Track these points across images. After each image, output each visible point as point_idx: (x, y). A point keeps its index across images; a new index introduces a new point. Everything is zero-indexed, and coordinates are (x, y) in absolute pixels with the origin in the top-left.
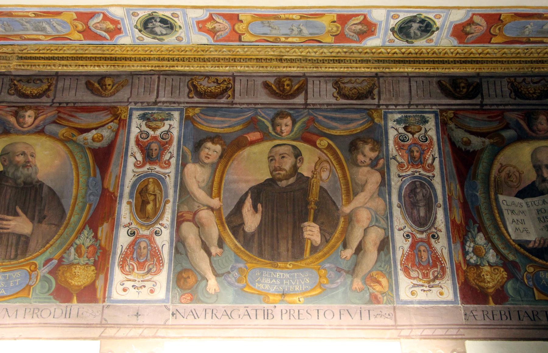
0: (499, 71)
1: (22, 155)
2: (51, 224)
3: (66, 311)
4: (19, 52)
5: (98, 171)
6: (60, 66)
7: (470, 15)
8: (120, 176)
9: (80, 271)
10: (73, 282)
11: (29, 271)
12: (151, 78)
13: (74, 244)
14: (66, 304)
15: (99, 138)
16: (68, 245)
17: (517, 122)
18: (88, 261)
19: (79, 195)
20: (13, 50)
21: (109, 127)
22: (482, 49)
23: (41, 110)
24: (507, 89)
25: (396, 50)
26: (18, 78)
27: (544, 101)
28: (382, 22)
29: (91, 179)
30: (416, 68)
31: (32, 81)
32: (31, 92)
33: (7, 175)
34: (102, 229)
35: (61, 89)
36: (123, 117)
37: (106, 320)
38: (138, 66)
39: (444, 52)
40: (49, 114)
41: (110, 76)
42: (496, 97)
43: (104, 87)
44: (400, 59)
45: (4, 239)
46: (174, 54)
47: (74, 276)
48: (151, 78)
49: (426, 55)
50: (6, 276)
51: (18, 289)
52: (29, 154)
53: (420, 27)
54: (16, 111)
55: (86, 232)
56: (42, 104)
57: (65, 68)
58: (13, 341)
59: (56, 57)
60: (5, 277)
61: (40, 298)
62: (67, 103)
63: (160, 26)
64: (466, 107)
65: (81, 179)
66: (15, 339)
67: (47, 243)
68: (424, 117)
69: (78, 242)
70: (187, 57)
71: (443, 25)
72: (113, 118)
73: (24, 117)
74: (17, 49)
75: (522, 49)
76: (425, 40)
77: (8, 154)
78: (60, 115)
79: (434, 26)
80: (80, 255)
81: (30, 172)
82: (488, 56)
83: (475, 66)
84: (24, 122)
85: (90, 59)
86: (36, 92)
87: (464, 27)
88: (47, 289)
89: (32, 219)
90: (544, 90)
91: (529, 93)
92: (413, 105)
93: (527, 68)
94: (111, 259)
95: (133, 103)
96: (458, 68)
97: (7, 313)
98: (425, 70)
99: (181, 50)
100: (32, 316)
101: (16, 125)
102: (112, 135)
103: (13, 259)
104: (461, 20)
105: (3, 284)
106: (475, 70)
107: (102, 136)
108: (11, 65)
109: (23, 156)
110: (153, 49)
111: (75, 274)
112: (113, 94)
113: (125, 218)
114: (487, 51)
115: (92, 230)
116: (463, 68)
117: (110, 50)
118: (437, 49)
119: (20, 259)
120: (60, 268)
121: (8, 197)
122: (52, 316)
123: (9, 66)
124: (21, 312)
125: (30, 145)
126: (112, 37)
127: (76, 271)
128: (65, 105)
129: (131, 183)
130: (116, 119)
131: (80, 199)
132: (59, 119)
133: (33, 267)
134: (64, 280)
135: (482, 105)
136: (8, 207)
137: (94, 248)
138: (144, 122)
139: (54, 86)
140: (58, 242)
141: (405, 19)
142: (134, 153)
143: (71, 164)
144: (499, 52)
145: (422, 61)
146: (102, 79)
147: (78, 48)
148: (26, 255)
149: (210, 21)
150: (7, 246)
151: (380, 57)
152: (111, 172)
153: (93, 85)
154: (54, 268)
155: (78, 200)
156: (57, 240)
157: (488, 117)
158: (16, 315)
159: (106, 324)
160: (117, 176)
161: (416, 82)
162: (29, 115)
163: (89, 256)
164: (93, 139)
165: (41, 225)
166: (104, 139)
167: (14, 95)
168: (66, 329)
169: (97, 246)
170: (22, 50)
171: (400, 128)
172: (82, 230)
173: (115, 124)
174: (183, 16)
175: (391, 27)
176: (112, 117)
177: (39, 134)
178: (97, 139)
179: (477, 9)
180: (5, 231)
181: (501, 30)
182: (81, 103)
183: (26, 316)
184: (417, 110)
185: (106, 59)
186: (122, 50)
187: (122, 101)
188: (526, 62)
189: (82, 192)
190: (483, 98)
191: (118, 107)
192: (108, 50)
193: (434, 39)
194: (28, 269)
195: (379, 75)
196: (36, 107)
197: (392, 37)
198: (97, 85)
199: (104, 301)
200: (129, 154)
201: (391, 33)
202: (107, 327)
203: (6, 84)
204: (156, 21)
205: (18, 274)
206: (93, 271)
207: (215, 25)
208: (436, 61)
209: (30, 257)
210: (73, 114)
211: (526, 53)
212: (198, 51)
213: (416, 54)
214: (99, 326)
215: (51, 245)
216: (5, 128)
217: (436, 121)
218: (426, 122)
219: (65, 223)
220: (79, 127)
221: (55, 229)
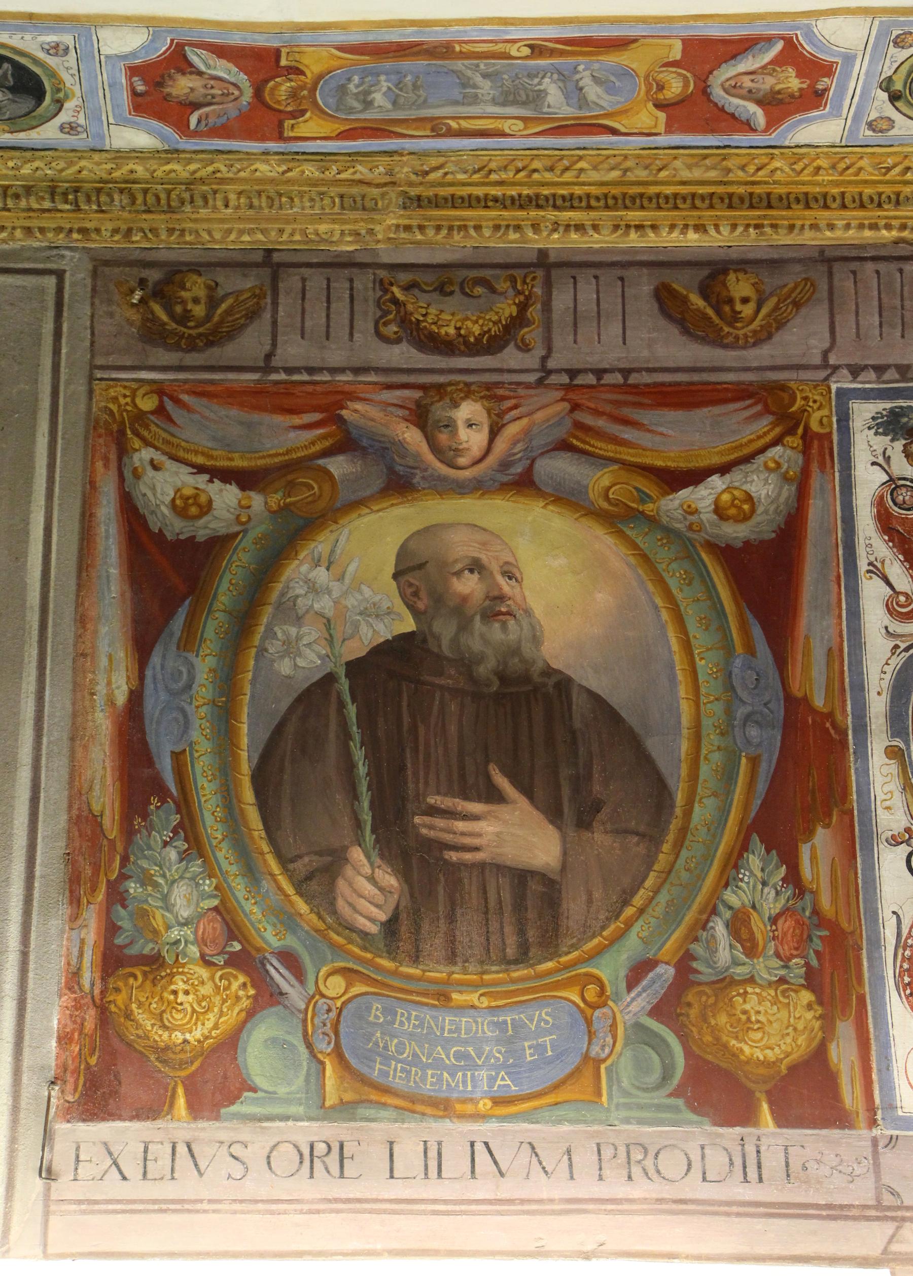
1: (471, 571)
2: (627, 832)
3: (744, 1156)
4: (413, 177)
5: (757, 632)
6: (555, 230)
8: (841, 650)
9: (761, 1009)
10: (747, 1050)
11: (582, 1005)
12: (901, 271)
13: (721, 907)
14: (738, 1130)
15: (739, 508)
16: (701, 912)
18: (782, 972)
19: (707, 722)
20: (390, 173)
21: (772, 465)
23: (508, 398)
26: (405, 277)
29: (738, 662)
31: (456, 288)
32: (458, 329)
33: (436, 650)
34: (813, 849)
35: (570, 319)
36: (815, 426)
37: (893, 1193)
38: (848, 227)
40: (539, 416)
41: (743, 265)
43: (727, 308)
45: (471, 886)
47: (745, 1025)
48: (901, 271)
50: (505, 1022)
51: (558, 1073)
52: (495, 568)
54: (418, 403)
55: (754, 861)
56: (507, 378)
57: (574, 236)
58: (581, 1263)
59: (547, 199)
60: (502, 1026)
61: (641, 1107)
62: (599, 373)
65: (700, 664)
66: (587, 1256)
67: (626, 903)
69: (730, 897)
72: (778, 430)
73: (450, 425)
74: (406, 170)
77: (421, 566)
78: (581, 416)
80: (751, 950)
81: (512, 638)
84: (454, 446)
85: (673, 202)
86: (476, 330)
88: (656, 1076)
89: (554, 814)
94: (865, 963)
95: (845, 372)
97: (534, 1159)
100: (625, 1173)
101: (429, 457)
102: (785, 493)
103: (516, 962)
105: (500, 1052)
107: (749, 498)
108: (378, 228)
109: (476, 576)
111: (749, 1020)
112: (763, 336)
113: (888, 808)
115: (774, 852)
117: (751, 169)
119: (540, 963)
120: (690, 997)
121: (453, 729)
122: (696, 1172)
123: (371, 232)
124: (585, 1158)
125: (492, 533)
126: (773, 123)
127: (747, 1007)
128: (591, 379)
129: (888, 677)
130: (791, 431)
131: (711, 739)
132: (580, 434)
133: (591, 992)
134: (710, 1039)
136: (462, 768)
137: (797, 922)
138: (899, 445)
139: (539, 306)
140: (663, 898)
142: (879, 565)
143: (656, 607)
146: (712, 276)
147: (629, 164)
148: (557, 946)
150: (486, 913)
152: (807, 637)
153: (685, 300)
154: (665, 994)
155: (704, 742)
156: (656, 892)
158: (571, 1166)
159: (899, 1208)
160: (830, 650)
162: (468, 420)
163: (785, 950)
164: (719, 511)
165: (587, 835)
166: (760, 510)
167: (398, 341)
168: (759, 1224)
169: (807, 913)
170: (427, 173)
172: (740, 856)
173: (789, 452)
176: (774, 425)
177: (519, 493)
178: (732, 511)
180: (468, 856)
182: (650, 370)
183: (606, 1172)
185: (731, 202)
186: (798, 167)
187: (804, 361)
189: (714, 711)
191: (792, 385)
194: (578, 1000)
196: (488, 389)
198: (697, 301)
199: (873, 1123)
200: (863, 565)
202: (904, 1219)
203: (366, 300)
205: (543, 1015)
206: (809, 1007)
209: (575, 954)
210: (628, 412)
214: (873, 1213)
215: (641, 911)
216: (391, 470)
219: (674, 826)
220: (659, 463)
221: (641, 849)
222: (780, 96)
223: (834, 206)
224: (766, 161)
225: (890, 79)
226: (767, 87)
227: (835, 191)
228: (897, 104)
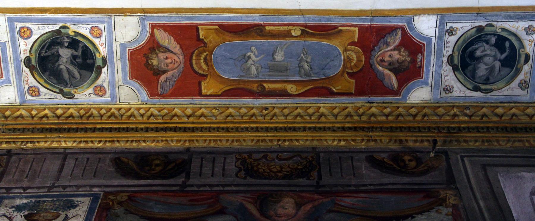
0: (224, 145)
7: (148, 29)
17: (242, 206)
22: (193, 109)
24: (234, 167)
25: (47, 112)
27: (295, 181)
28: (5, 43)
30: (80, 142)
39: (129, 113)
42: (212, 176)
44: (52, 126)
49: (98, 120)
53: (74, 57)
64: (153, 188)
68: (73, 201)
71: (111, 51)
75: (257, 108)
76: (90, 90)
79: (97, 55)
82: (203, 119)
83: (183, 137)
87: (146, 56)
90: (296, 169)
91: (271, 171)
92: (59, 186)
93: (271, 141)
96: (154, 141)
98: (97, 145)
104: (136, 40)
106: (182, 142)
114: (201, 111)
116: (162, 141)
118: (116, 109)
135: (184, 185)
141: (44, 37)
144: (221, 113)
145: (91, 129)
151: (17, 124)
157: (190, 201)
161: (77, 159)
171: (19, 217)
175: (23, 57)
179: (155, 15)
181: (209, 64)
184: (64, 193)
188: (267, 130)
190: (188, 177)
193: (105, 85)
195: (12, 153)
197: (32, 81)
201: (27, 70)
208: (116, 129)
211: (265, 116)
213: (81, 117)
217: (91, 204)
218: (72, 206)
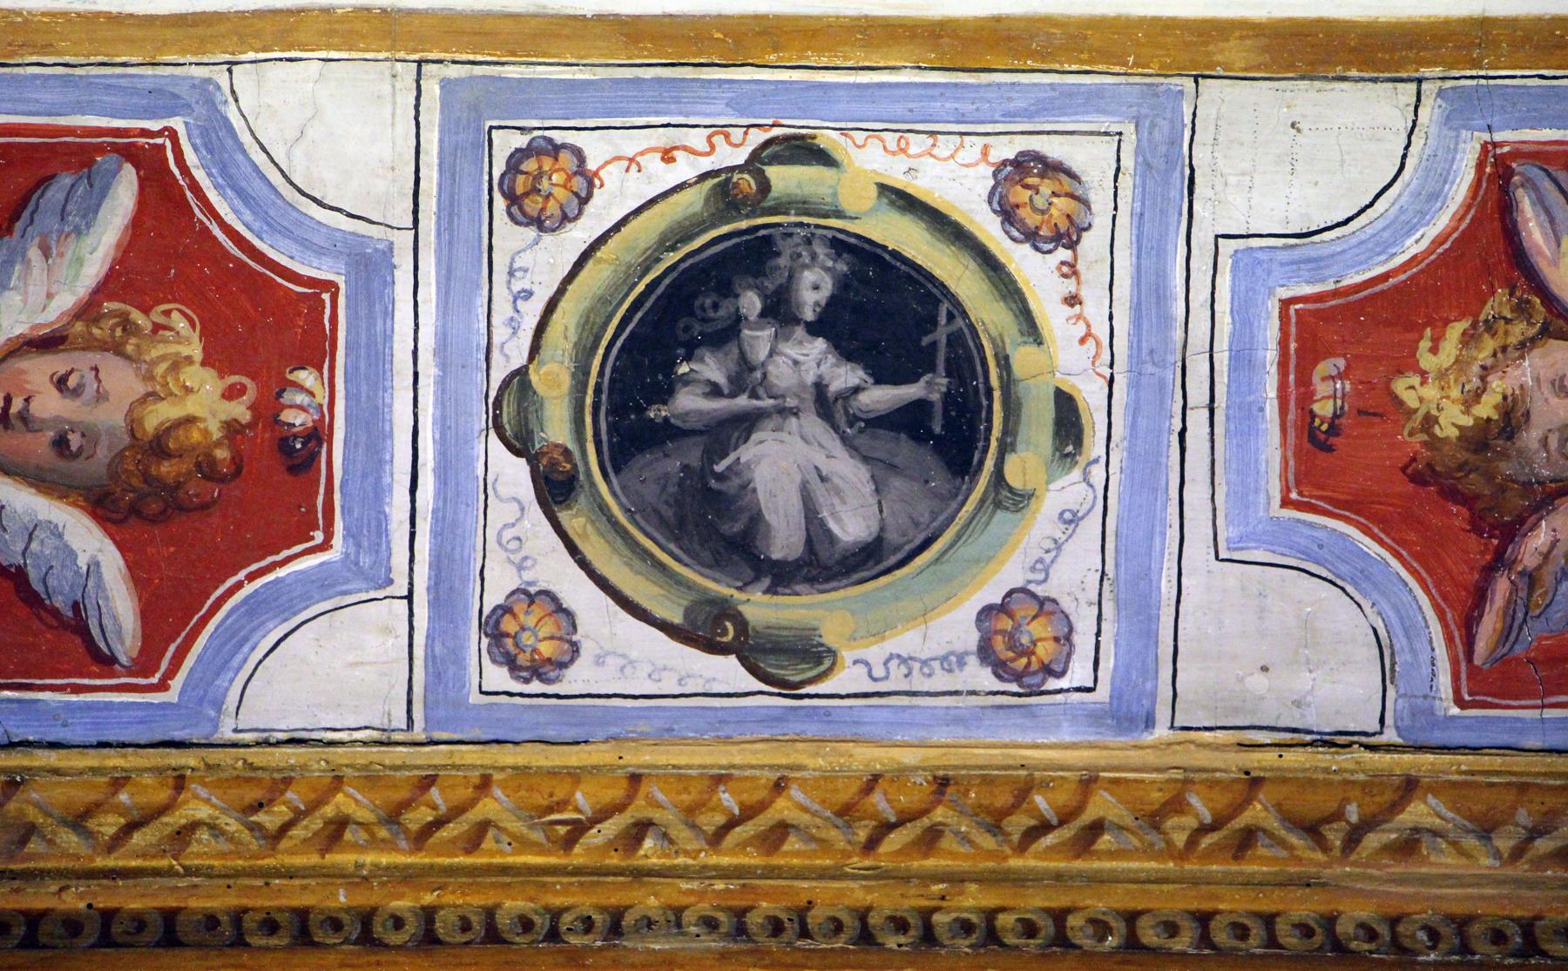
46: (931, 863)
63: (825, 403)
70: (1099, 903)
99: (1018, 823)
110: (659, 803)
117: (108, 825)
149: (1470, 309)
174: (1139, 218)
186: (269, 819)
192: (78, 820)
204: (779, 310)
207: (1526, 372)
212: (1247, 840)
222: (166, 469)
223: (396, 938)
224: (163, 795)
225: (519, 378)
226: (111, 417)
227: (403, 904)
228: (564, 516)
